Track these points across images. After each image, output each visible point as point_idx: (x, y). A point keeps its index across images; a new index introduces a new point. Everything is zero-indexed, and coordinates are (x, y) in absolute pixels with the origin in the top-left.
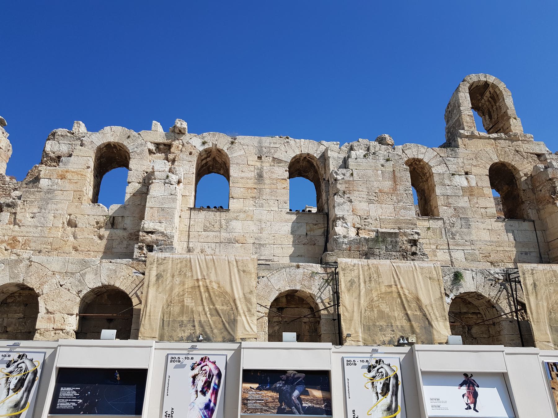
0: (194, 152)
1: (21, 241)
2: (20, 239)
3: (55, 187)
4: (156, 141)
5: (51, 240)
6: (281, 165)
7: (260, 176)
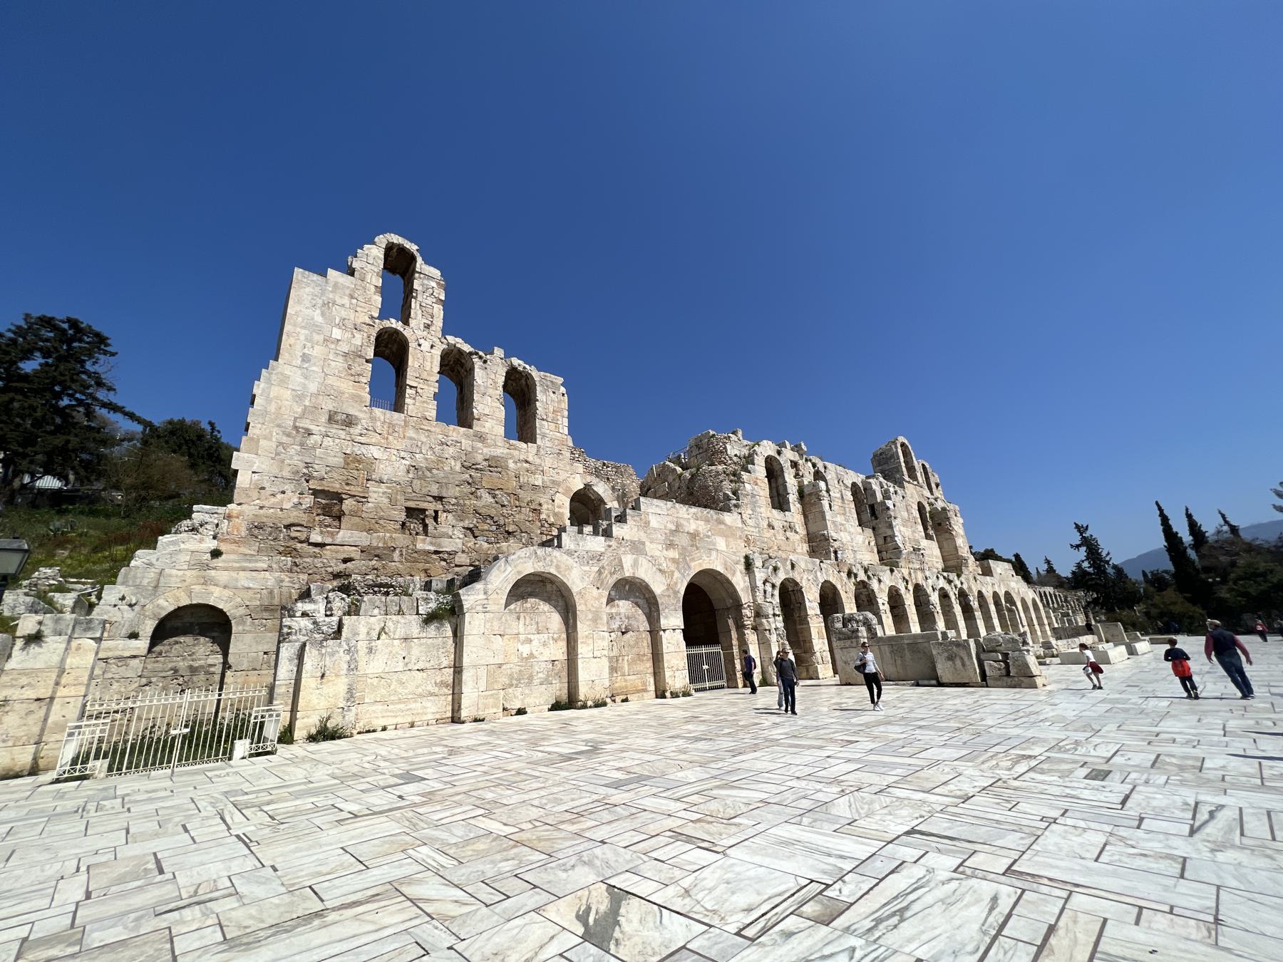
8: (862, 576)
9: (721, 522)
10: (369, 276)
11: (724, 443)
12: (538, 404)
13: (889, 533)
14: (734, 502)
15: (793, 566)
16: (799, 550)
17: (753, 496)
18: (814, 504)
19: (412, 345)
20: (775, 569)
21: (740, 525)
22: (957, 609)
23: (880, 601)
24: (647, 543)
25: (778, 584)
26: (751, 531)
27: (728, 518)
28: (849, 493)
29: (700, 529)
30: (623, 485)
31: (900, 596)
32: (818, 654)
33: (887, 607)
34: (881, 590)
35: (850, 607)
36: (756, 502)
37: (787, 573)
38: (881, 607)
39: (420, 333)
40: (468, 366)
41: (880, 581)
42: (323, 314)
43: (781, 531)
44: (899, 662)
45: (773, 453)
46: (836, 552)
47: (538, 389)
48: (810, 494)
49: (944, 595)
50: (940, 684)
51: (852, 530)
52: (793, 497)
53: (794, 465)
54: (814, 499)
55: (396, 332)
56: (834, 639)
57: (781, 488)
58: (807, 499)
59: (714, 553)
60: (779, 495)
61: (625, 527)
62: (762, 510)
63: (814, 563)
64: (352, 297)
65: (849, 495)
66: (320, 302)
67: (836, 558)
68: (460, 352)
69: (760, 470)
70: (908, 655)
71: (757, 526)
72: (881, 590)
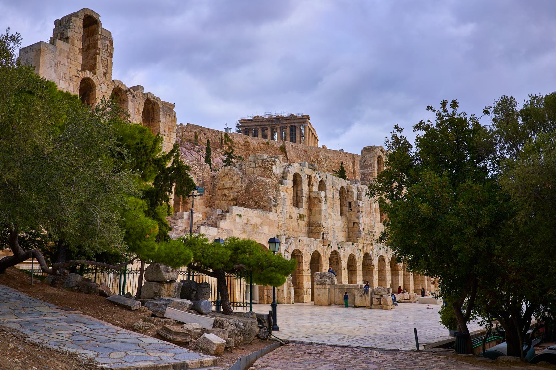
3: (285, 197)
9: (267, 218)
10: (76, 41)
11: (272, 165)
12: (161, 124)
13: (357, 221)
14: (274, 203)
17: (284, 199)
18: (316, 204)
19: (98, 88)
21: (277, 219)
22: (388, 268)
23: (343, 262)
24: (234, 231)
25: (291, 252)
27: (272, 216)
28: (338, 194)
30: (203, 177)
31: (355, 259)
32: (305, 290)
35: (325, 267)
37: (296, 247)
38: (343, 266)
39: (102, 80)
40: (124, 97)
42: (55, 72)
43: (296, 219)
46: (323, 234)
47: (161, 113)
48: (315, 198)
49: (382, 259)
50: (356, 307)
51: (335, 218)
52: (304, 199)
55: (88, 79)
56: (315, 284)
57: (299, 192)
60: (297, 196)
61: (226, 222)
62: (288, 207)
63: (311, 241)
64: (68, 58)
65: (337, 196)
66: (54, 63)
68: (120, 90)
69: (289, 182)
72: (344, 256)
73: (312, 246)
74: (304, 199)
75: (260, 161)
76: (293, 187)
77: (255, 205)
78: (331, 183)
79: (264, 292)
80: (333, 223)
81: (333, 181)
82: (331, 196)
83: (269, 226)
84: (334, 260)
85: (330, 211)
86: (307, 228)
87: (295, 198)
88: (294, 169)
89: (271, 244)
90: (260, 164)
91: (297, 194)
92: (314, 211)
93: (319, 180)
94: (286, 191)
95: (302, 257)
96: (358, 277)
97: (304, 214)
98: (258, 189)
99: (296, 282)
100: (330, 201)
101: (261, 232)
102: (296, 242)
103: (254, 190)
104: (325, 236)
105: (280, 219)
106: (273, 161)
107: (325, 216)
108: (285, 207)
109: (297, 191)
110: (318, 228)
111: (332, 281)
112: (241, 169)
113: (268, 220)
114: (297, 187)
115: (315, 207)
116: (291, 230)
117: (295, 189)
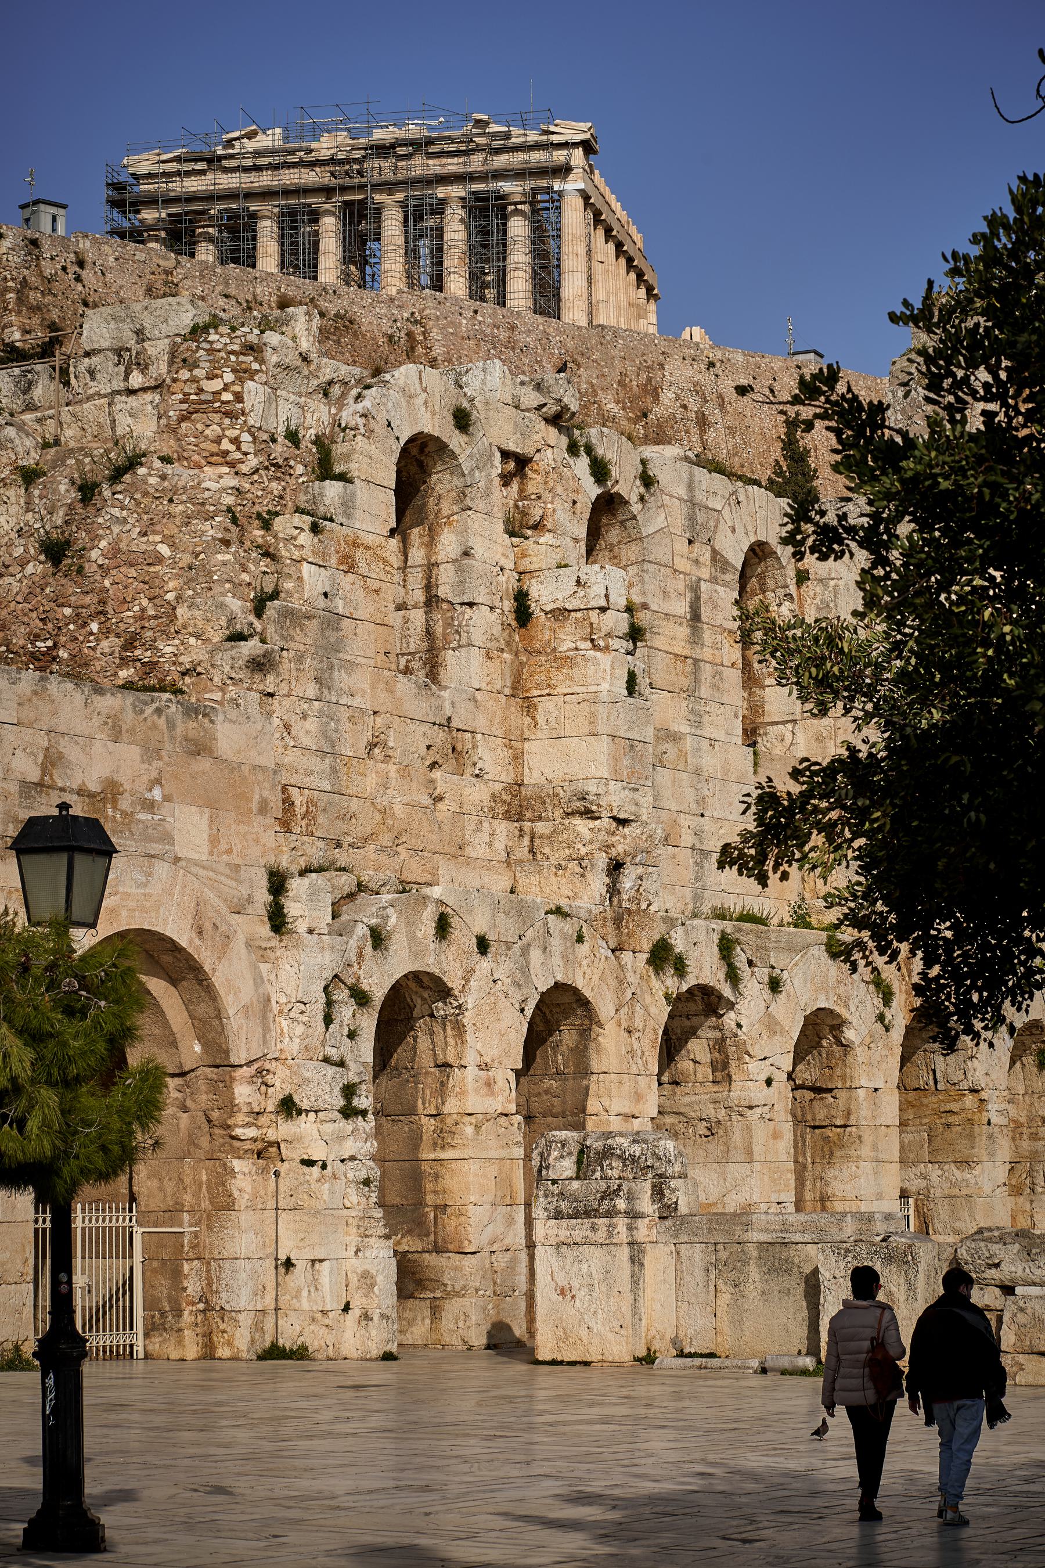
0: (580, 498)
1: (297, 803)
2: (294, 792)
3: (340, 606)
4: (512, 447)
5: (355, 805)
6: (728, 577)
7: (696, 617)
8: (705, 968)
9: (199, 748)
11: (243, 374)
14: (250, 648)
15: (443, 927)
16: (478, 849)
17: (332, 620)
20: (378, 938)
25: (379, 992)
26: (311, 774)
29: (124, 779)
33: (781, 1093)
34: (771, 1025)
36: (336, 648)
41: (775, 985)
43: (419, 768)
44: (725, 1298)
45: (435, 423)
46: (616, 867)
48: (560, 614)
51: (709, 762)
53: (518, 465)
54: (567, 639)
56: (539, 1213)
58: (542, 627)
59: (162, 869)
60: (432, 601)
67: (613, 890)
70: (754, 1273)
71: (329, 750)
72: (771, 1025)
73: (536, 955)
74: (485, 623)
75: (157, 349)
76: (399, 531)
77: (124, 662)
78: (678, 513)
79: (177, 1275)
80: (690, 795)
81: (692, 502)
82: (681, 607)
83: (211, 804)
84: (698, 1048)
85: (668, 710)
86: (503, 828)
87: (418, 616)
88: (411, 401)
89: (37, 862)
90: (160, 369)
91: (429, 587)
92: (546, 707)
93: (594, 491)
94: (349, 566)
95: (460, 1030)
96: (867, 1167)
97: (481, 723)
98: (141, 545)
99: (420, 1204)
100: (669, 637)
101: (156, 848)
102: (411, 924)
103: (115, 551)
104: (627, 883)
105: (291, 757)
106: (250, 349)
107: (631, 744)
108: (342, 679)
109: (431, 567)
110: (582, 826)
111: (658, 1192)
112: (30, 407)
113: (204, 764)
114: (431, 544)
115: (557, 677)
116: (386, 839)
117: (417, 555)
